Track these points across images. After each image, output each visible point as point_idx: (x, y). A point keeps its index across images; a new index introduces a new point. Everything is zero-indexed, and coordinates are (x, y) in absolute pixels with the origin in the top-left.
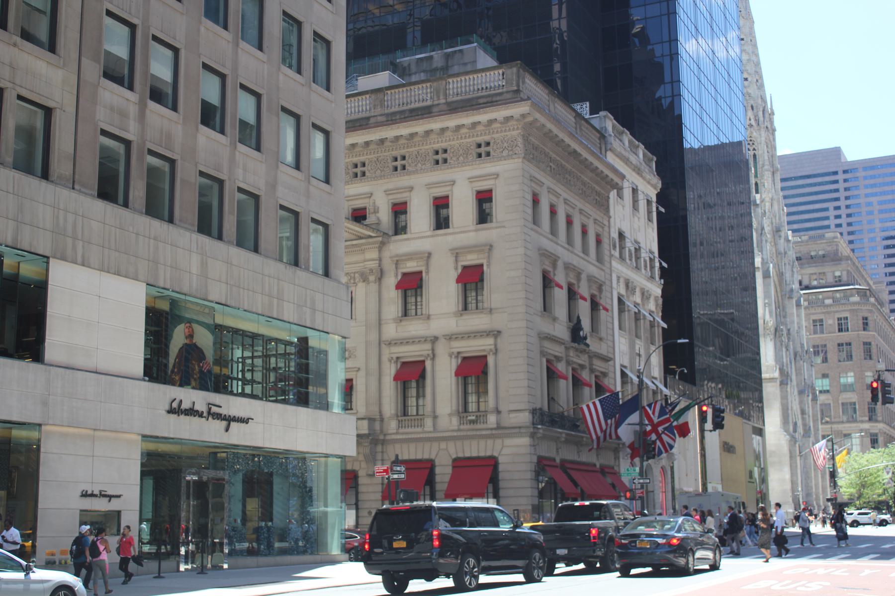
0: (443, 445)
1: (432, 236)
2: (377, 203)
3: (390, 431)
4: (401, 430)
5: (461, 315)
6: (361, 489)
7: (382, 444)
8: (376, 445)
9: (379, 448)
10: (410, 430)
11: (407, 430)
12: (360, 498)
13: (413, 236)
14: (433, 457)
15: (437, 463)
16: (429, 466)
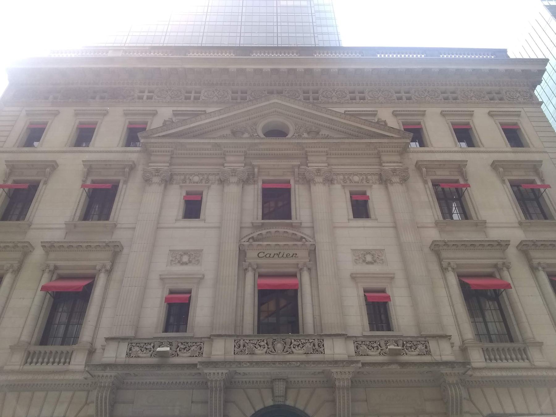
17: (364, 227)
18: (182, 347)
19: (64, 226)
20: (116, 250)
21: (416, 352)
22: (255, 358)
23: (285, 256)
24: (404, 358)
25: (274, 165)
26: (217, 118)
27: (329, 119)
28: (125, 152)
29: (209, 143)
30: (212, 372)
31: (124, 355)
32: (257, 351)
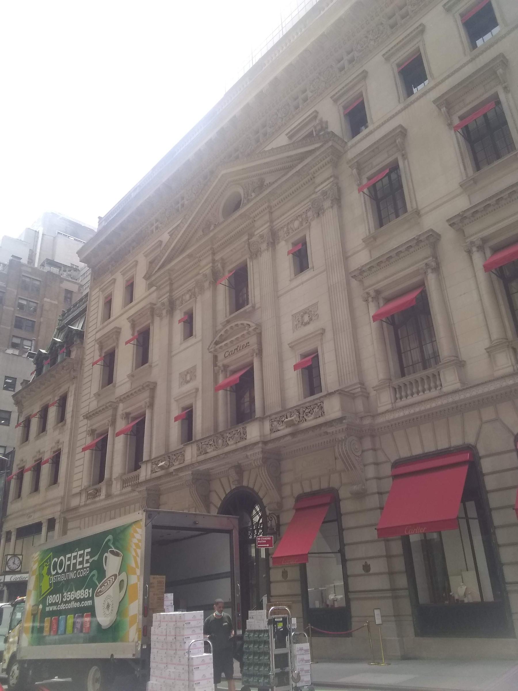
0: (488, 413)
1: (405, 108)
2: (324, 119)
3: (381, 410)
4: (400, 403)
5: (475, 181)
6: (348, 522)
7: (373, 436)
8: (361, 438)
9: (367, 443)
10: (416, 398)
11: (410, 400)
12: (347, 540)
13: (376, 125)
14: (471, 440)
15: (482, 452)
16: (467, 457)
17: (302, 283)
18: (174, 458)
19: (127, 379)
20: (152, 388)
21: (313, 416)
22: (208, 456)
23: (241, 348)
24: (304, 425)
25: (232, 251)
26: (186, 225)
27: (264, 163)
28: (150, 294)
29: (184, 258)
30: (184, 474)
31: (149, 472)
32: (208, 451)
